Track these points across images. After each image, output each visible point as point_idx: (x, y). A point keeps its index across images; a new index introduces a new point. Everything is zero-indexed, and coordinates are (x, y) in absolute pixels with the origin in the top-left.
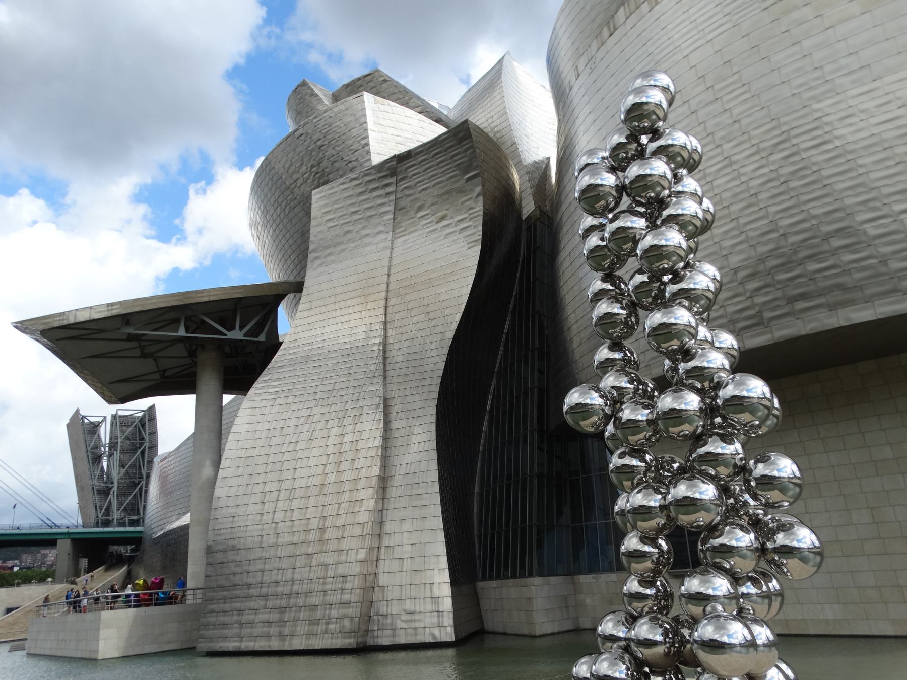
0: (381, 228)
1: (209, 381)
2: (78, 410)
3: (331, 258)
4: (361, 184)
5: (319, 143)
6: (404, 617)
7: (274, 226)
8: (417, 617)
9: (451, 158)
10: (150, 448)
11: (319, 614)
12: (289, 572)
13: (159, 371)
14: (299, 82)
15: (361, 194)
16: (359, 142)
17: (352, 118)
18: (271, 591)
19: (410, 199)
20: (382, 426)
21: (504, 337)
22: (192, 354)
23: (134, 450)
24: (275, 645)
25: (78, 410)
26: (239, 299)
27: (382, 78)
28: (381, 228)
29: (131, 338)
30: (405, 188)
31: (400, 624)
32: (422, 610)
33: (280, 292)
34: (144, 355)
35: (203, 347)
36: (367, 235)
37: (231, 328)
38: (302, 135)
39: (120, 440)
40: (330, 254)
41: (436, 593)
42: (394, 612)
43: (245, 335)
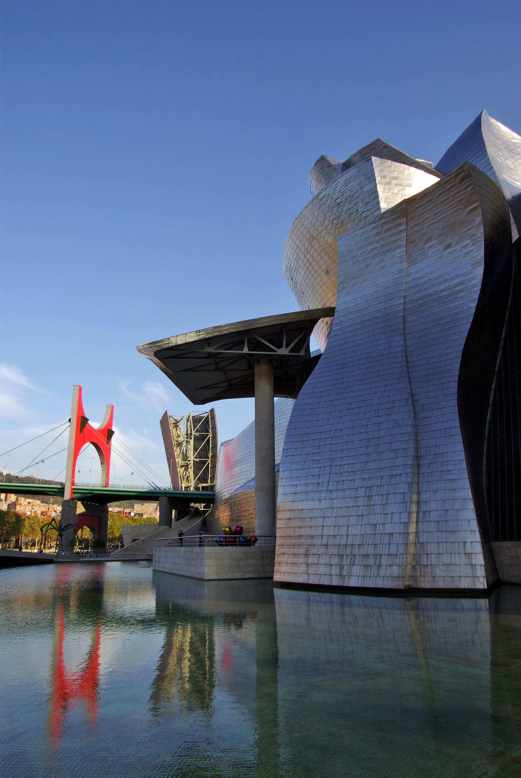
1: (263, 386)
2: (166, 413)
4: (378, 226)
5: (338, 201)
6: (441, 567)
7: (305, 269)
8: (453, 568)
9: (454, 196)
10: (212, 438)
11: (371, 561)
12: (345, 528)
13: (227, 381)
14: (318, 157)
18: (331, 542)
19: (419, 233)
20: (412, 415)
21: (502, 342)
22: (251, 367)
23: (203, 438)
24: (335, 582)
25: (166, 413)
26: (285, 324)
29: (210, 355)
30: (415, 226)
31: (438, 572)
32: (458, 563)
33: (315, 318)
34: (217, 369)
35: (259, 362)
37: (280, 347)
38: (324, 197)
39: (193, 432)
41: (469, 550)
42: (433, 563)
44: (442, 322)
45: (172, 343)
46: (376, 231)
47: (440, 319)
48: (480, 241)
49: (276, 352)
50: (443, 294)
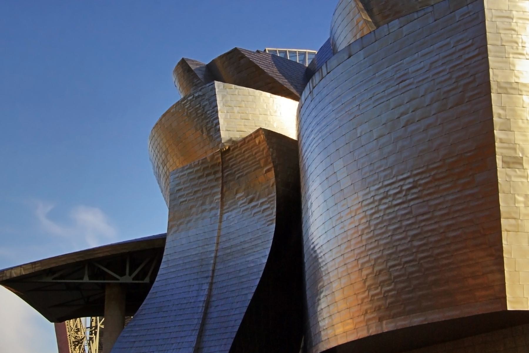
0: (213, 205)
3: (182, 227)
15: (200, 178)
16: (212, 122)
17: (207, 102)
27: (240, 56)
28: (213, 205)
30: (228, 175)
36: (203, 211)
37: (122, 274)
40: (180, 224)
43: (133, 279)
44: (241, 274)
45: (6, 276)
46: (200, 174)
47: (240, 271)
48: (273, 200)
49: (118, 280)
50: (246, 246)
